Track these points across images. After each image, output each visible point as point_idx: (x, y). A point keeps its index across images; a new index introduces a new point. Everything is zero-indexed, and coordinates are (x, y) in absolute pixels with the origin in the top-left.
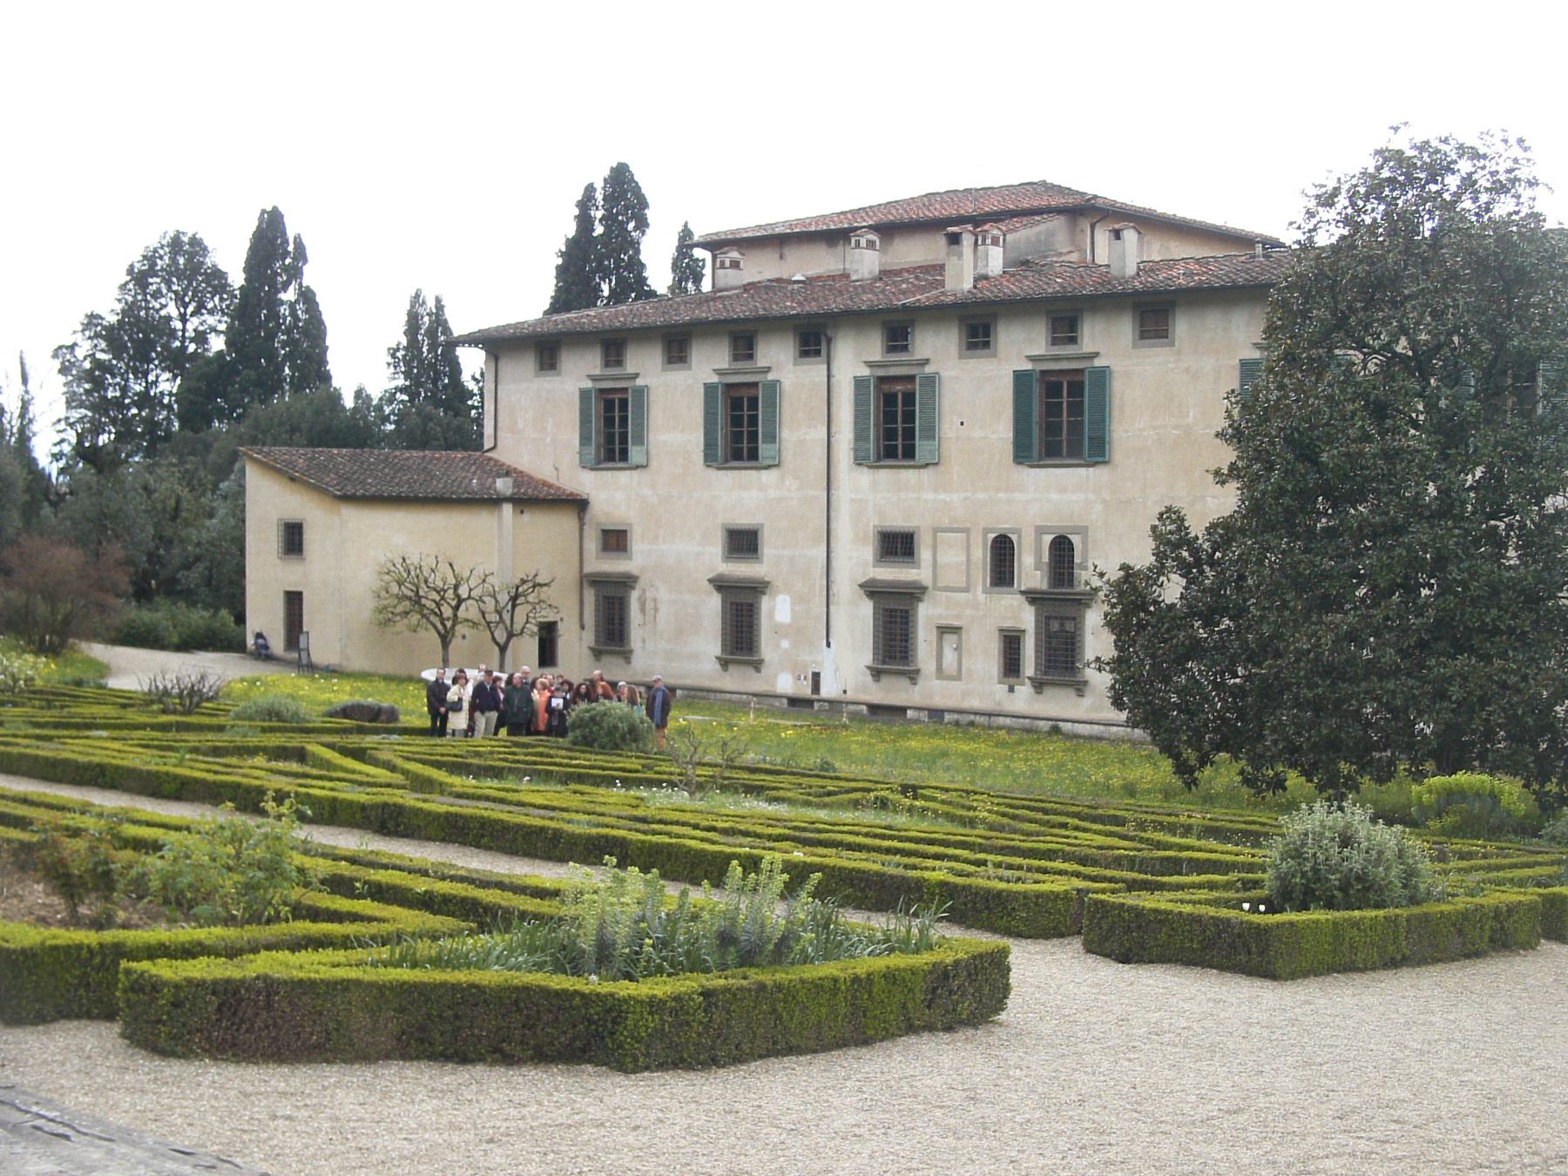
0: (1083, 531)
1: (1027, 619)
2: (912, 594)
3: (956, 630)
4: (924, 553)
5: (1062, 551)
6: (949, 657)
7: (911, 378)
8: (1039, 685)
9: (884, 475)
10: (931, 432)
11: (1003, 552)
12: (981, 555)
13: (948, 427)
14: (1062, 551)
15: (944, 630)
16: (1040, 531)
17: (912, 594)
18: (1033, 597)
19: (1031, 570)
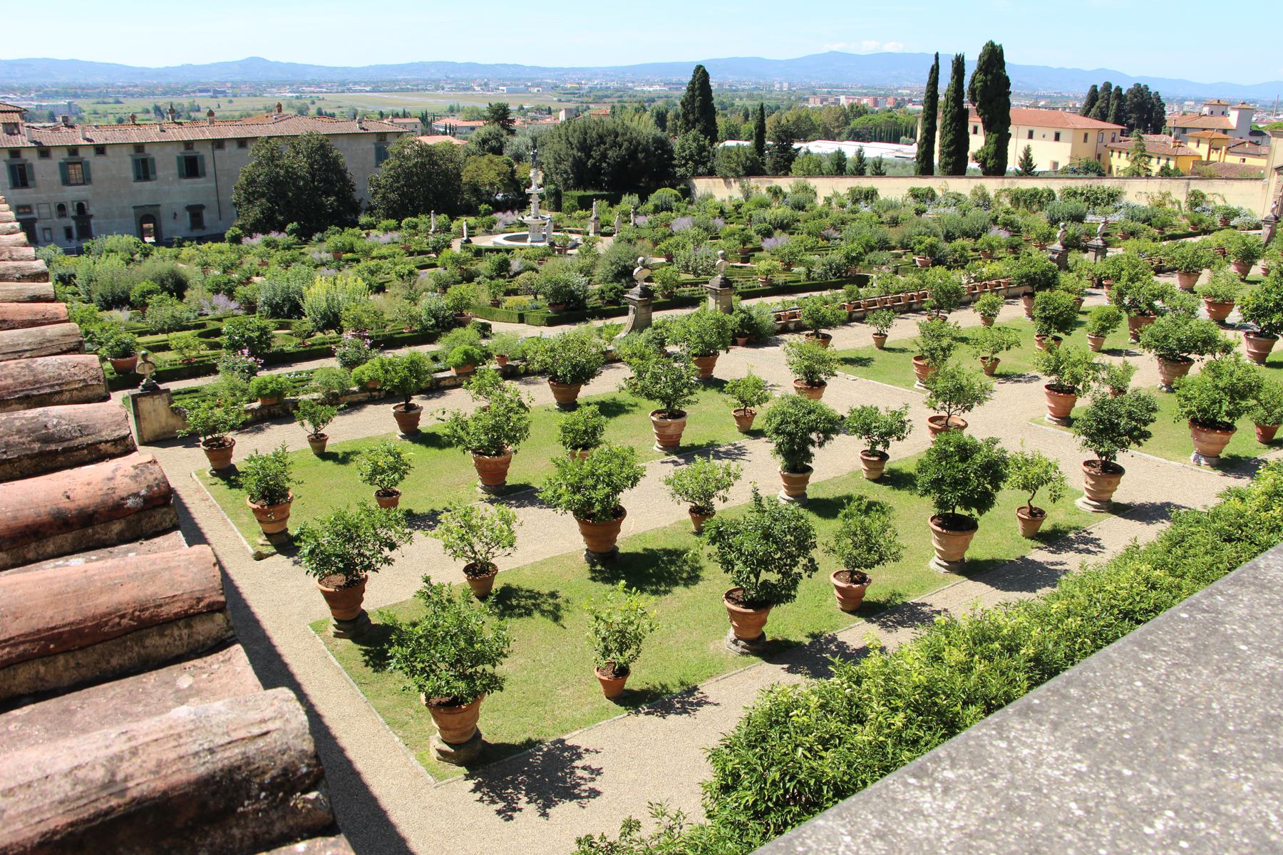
0: (87, 201)
1: (73, 223)
2: (34, 220)
3: (49, 229)
4: (35, 211)
5: (81, 208)
6: (48, 236)
7: (23, 165)
8: (79, 239)
9: (16, 191)
10: (33, 179)
11: (61, 208)
12: (54, 209)
13: (38, 177)
14: (81, 208)
15: (44, 229)
16: (73, 202)
17: (34, 220)
18: (73, 218)
19: (71, 211)
